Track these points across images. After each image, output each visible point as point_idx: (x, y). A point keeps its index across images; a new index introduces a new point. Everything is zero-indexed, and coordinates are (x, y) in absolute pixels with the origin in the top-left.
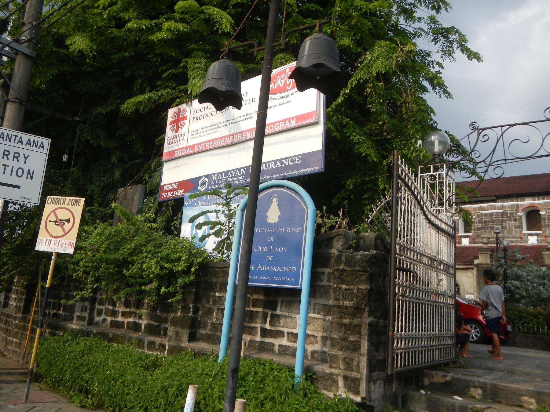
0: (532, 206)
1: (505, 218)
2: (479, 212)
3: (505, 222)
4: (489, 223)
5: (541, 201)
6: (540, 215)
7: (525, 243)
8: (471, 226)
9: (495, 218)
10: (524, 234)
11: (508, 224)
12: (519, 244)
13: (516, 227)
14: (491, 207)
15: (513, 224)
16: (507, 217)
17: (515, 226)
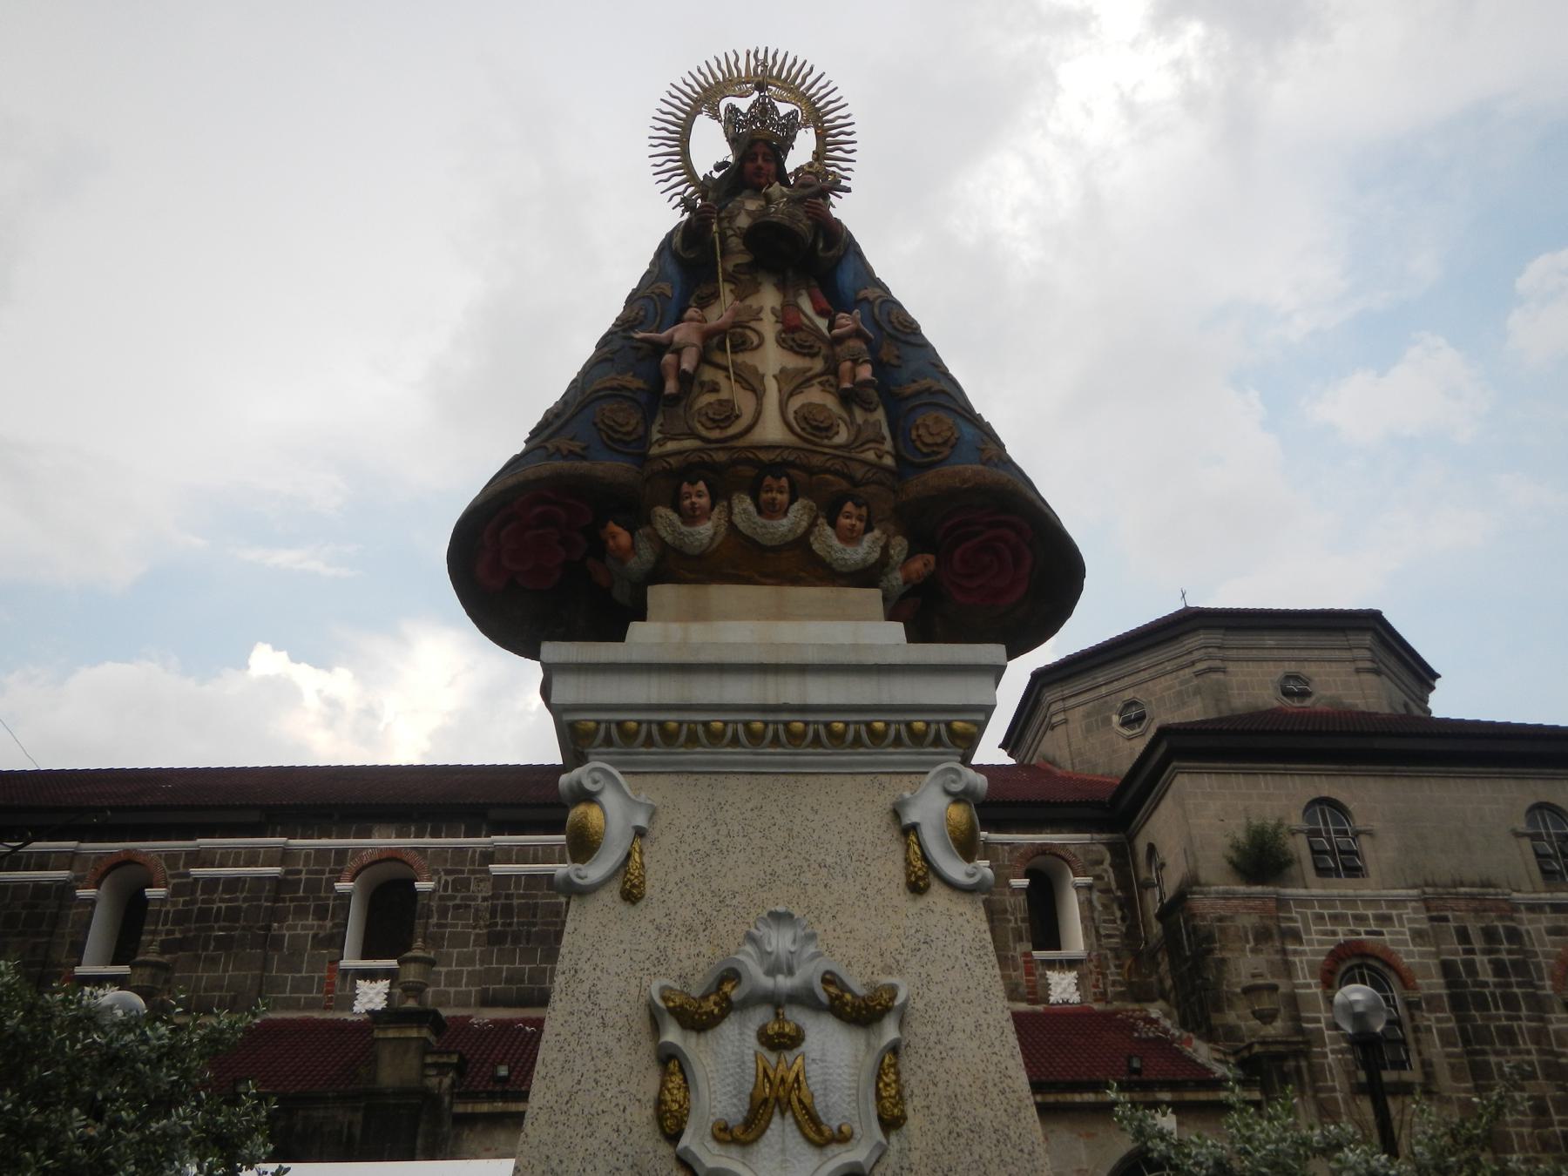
0: (392, 857)
1: (284, 900)
2: (188, 875)
3: (282, 920)
4: (217, 921)
5: (427, 841)
6: (415, 894)
7: (343, 1010)
8: (141, 934)
9: (245, 900)
10: (345, 972)
11: (289, 928)
12: (316, 1015)
13: (319, 942)
14: (238, 855)
15: (312, 927)
16: (292, 900)
17: (315, 936)
